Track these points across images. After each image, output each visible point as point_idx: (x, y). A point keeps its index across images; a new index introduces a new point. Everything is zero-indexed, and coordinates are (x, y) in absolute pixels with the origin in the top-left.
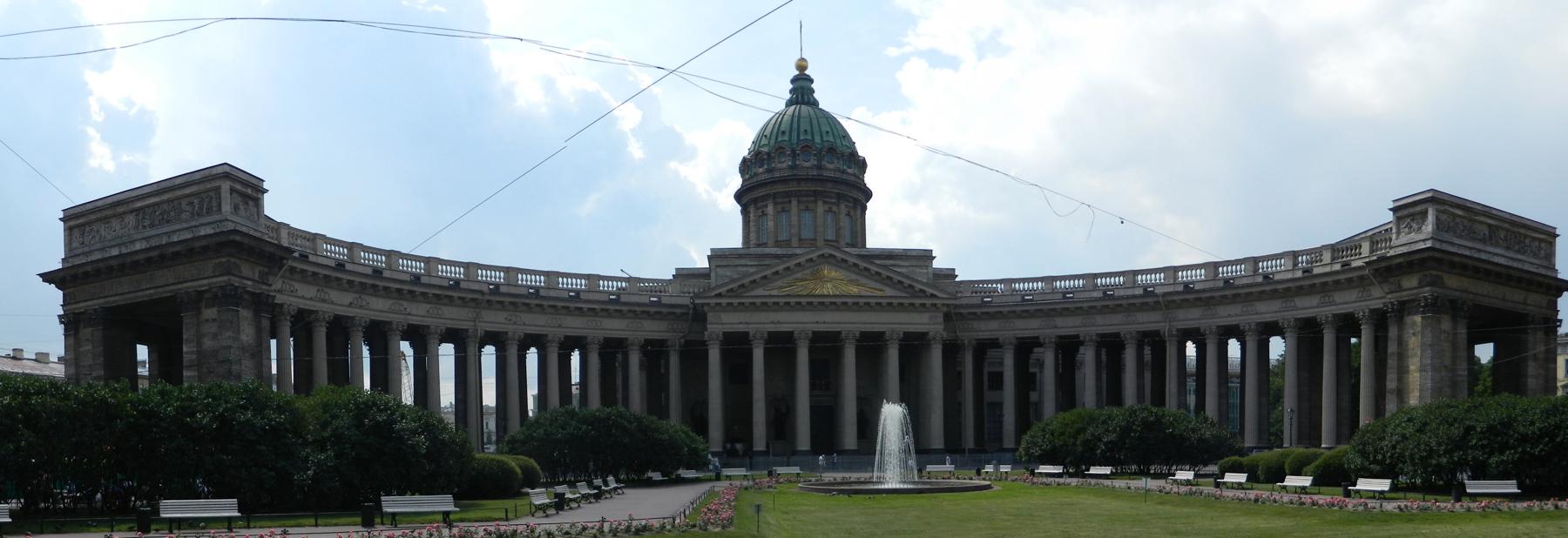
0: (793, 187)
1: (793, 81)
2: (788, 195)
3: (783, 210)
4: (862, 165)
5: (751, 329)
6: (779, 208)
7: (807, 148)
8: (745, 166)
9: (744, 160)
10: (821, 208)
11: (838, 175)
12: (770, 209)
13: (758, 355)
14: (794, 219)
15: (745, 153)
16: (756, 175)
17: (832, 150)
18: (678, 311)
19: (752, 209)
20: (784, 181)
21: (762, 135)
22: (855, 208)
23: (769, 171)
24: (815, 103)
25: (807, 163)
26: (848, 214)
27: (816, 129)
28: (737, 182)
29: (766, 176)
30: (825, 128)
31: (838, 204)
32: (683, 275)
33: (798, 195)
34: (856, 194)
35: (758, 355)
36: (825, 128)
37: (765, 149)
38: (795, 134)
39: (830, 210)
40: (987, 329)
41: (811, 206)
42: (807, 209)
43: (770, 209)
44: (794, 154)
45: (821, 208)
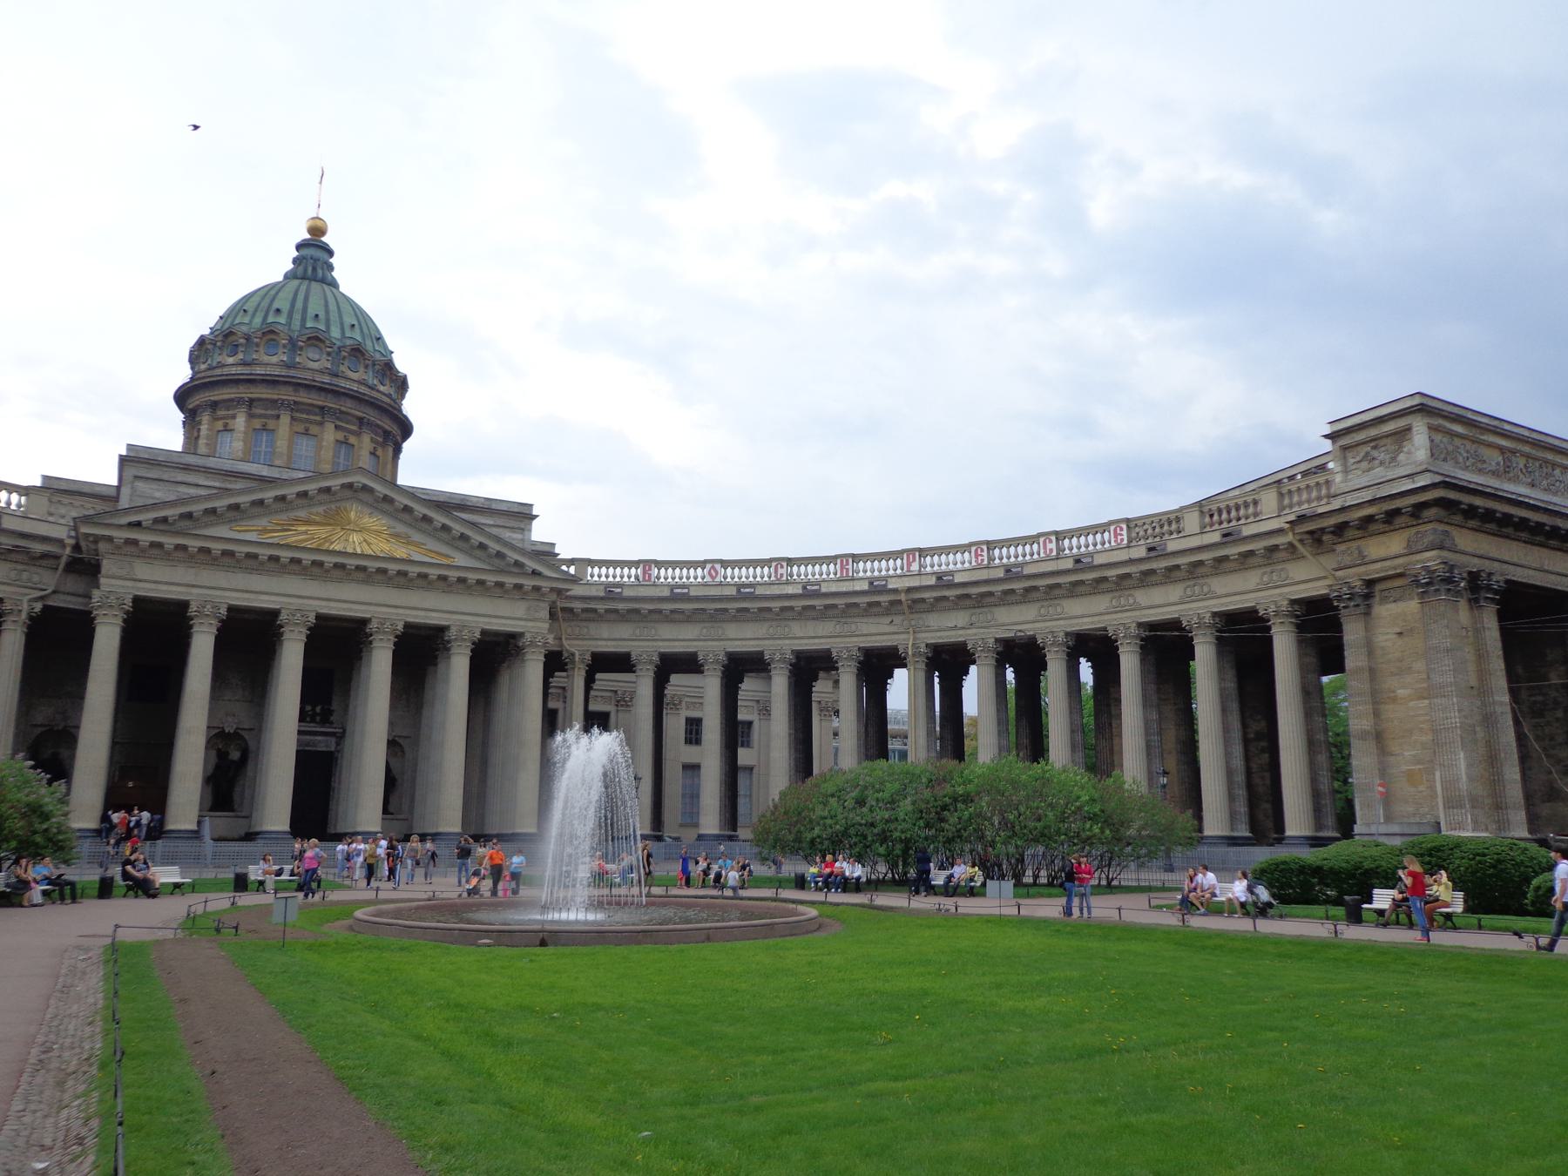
0: (286, 394)
1: (299, 247)
2: (273, 403)
3: (264, 428)
4: (402, 385)
5: (193, 596)
6: (257, 423)
7: (316, 340)
8: (201, 350)
9: (202, 342)
10: (330, 434)
11: (363, 389)
12: (240, 422)
13: (202, 648)
14: (281, 444)
15: (207, 332)
16: (221, 365)
17: (357, 352)
18: (38, 548)
19: (205, 418)
20: (271, 382)
21: (240, 308)
22: (384, 445)
23: (244, 364)
24: (334, 284)
25: (314, 363)
26: (373, 454)
27: (334, 316)
28: (182, 373)
29: (240, 370)
30: (349, 320)
31: (358, 434)
32: (55, 490)
33: (295, 407)
34: (387, 424)
35: (202, 648)
36: (349, 320)
37: (244, 329)
38: (297, 317)
39: (345, 442)
40: (610, 639)
41: (314, 429)
42: (306, 433)
43: (240, 422)
44: (293, 346)
45: (330, 434)
